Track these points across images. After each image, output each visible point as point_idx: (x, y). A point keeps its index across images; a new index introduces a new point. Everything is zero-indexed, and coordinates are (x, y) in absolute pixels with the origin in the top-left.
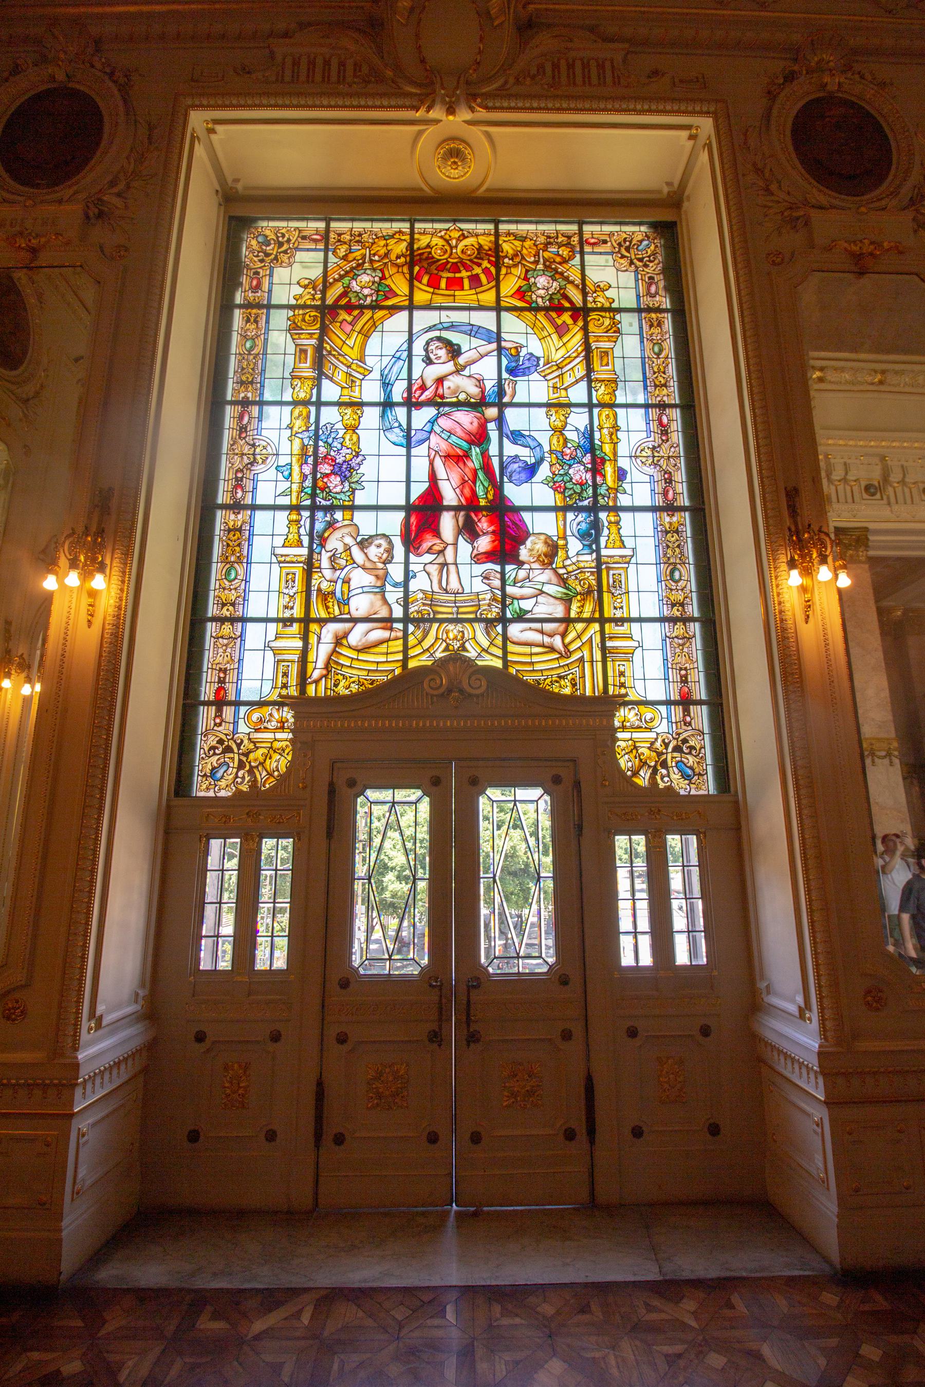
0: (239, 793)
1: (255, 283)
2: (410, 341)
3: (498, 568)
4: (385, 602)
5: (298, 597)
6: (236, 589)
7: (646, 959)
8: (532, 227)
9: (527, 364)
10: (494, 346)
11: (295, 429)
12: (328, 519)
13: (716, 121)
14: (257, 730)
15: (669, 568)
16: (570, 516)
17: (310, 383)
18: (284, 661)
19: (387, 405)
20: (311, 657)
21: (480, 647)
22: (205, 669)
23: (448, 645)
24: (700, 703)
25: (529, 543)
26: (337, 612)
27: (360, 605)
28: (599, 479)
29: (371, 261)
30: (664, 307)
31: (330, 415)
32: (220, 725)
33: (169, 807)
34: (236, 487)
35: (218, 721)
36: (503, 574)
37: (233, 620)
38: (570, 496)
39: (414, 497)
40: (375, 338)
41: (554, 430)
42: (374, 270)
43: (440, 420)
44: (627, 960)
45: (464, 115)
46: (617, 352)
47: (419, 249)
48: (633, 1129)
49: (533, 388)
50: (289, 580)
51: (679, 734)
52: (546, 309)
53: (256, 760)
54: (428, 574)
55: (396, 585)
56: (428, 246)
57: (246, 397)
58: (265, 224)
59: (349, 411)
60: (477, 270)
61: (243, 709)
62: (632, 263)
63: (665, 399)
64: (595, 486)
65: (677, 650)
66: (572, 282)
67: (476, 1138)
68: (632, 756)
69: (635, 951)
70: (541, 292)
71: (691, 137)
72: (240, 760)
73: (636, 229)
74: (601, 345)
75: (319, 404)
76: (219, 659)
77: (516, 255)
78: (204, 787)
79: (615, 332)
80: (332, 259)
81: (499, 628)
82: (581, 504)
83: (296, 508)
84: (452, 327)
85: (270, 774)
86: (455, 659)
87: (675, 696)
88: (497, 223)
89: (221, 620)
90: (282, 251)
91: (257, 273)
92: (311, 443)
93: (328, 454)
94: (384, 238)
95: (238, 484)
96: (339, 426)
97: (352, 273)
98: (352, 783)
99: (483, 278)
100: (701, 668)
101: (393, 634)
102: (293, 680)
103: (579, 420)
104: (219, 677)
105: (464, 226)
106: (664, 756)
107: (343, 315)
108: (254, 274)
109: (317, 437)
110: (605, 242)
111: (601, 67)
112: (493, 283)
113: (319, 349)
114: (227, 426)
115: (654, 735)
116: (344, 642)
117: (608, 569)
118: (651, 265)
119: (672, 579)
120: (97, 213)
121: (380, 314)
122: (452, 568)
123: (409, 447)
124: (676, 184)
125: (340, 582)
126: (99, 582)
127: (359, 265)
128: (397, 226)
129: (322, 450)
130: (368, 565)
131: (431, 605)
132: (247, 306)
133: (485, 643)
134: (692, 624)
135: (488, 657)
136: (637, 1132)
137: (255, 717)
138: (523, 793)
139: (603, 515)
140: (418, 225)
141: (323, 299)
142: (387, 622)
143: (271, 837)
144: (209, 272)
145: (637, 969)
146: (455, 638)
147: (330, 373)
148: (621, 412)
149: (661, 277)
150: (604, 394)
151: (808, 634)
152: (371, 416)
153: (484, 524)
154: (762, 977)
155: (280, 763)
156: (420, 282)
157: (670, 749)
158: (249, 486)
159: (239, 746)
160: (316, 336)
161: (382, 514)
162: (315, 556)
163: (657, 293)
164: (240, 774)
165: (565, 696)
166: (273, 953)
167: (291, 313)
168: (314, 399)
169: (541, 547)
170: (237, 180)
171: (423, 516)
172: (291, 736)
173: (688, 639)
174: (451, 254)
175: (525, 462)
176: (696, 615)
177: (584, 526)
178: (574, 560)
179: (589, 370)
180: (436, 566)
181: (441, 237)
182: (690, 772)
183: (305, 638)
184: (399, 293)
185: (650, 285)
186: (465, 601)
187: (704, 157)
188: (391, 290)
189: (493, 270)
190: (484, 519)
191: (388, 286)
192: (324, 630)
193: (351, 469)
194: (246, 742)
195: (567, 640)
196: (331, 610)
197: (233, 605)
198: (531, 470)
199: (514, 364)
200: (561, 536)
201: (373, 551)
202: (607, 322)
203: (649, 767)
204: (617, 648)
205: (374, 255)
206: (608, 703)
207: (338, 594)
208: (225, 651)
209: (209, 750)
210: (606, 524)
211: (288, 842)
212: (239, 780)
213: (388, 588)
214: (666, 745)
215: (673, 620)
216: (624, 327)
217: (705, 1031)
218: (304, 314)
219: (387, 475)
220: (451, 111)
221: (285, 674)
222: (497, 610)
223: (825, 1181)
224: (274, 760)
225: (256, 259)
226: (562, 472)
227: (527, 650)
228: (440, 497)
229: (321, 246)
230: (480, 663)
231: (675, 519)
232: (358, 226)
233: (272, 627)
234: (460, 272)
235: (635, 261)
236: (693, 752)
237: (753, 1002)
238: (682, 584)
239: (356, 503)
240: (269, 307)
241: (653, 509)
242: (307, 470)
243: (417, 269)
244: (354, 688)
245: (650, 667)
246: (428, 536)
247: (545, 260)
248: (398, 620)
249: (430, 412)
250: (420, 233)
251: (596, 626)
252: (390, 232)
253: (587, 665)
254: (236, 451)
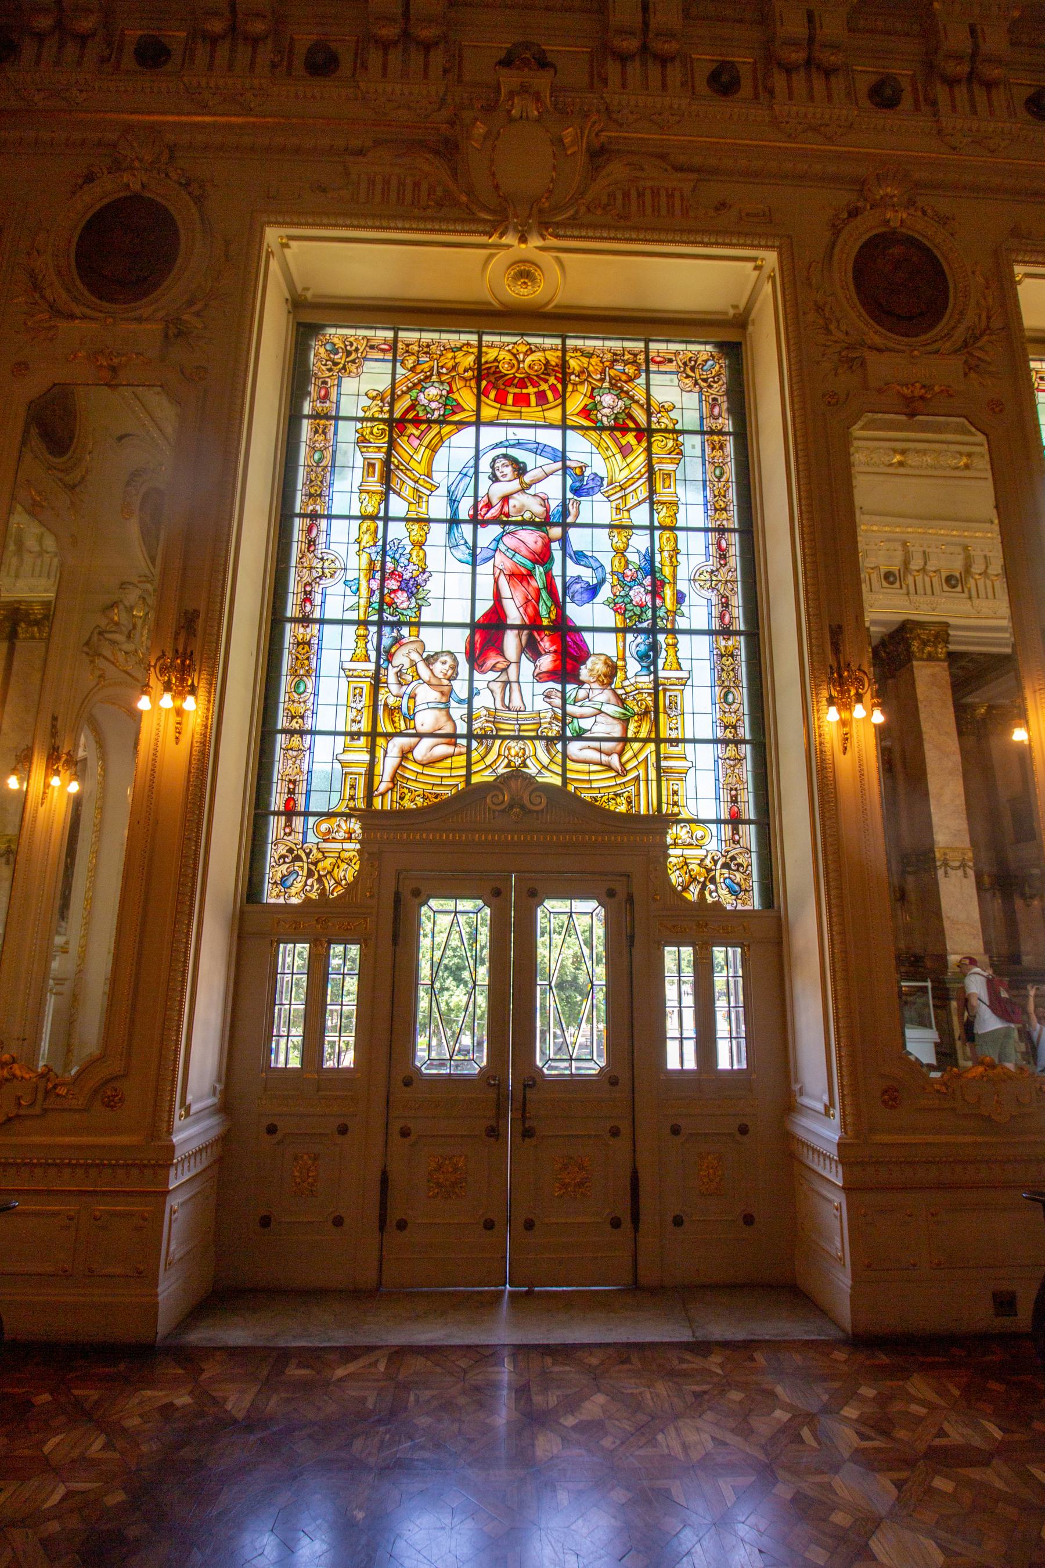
0: (308, 900)
1: (323, 393)
2: (477, 458)
3: (559, 687)
4: (450, 718)
5: (365, 711)
6: (305, 702)
7: (691, 1064)
8: (598, 343)
9: (591, 484)
10: (559, 465)
11: (363, 544)
12: (395, 634)
13: (780, 255)
14: (325, 841)
15: (725, 689)
16: (630, 637)
17: (378, 497)
18: (351, 773)
19: (454, 522)
20: (378, 770)
21: (541, 766)
22: (275, 780)
23: (510, 761)
24: (749, 822)
25: (589, 663)
26: (403, 727)
27: (426, 720)
28: (658, 601)
29: (439, 374)
30: (727, 430)
31: (397, 531)
32: (290, 834)
33: (242, 912)
34: (305, 600)
35: (288, 830)
36: (563, 692)
37: (302, 733)
38: (630, 618)
39: (479, 615)
40: (442, 452)
41: (617, 551)
42: (442, 383)
43: (504, 539)
44: (673, 1063)
45: (535, 242)
46: (679, 475)
47: (486, 363)
48: (675, 1217)
49: (596, 509)
50: (357, 694)
51: (728, 852)
52: (611, 429)
53: (324, 869)
54: (492, 692)
55: (460, 702)
56: (496, 360)
57: (314, 510)
58: (332, 331)
59: (416, 527)
60: (544, 387)
61: (312, 820)
62: (696, 383)
63: (725, 523)
64: (655, 609)
65: (729, 771)
66: (637, 402)
67: (529, 1225)
68: (682, 872)
69: (680, 1055)
70: (607, 411)
71: (756, 268)
72: (309, 869)
73: (701, 347)
74: (664, 466)
75: (387, 519)
76: (289, 771)
77: (583, 372)
78: (275, 894)
79: (678, 454)
80: (400, 370)
81: (559, 746)
82: (640, 626)
83: (365, 623)
84: (518, 445)
85: (338, 883)
86: (517, 775)
87: (725, 815)
88: (564, 338)
89: (291, 732)
90: (350, 360)
91: (326, 383)
92: (379, 558)
93: (395, 570)
94: (452, 350)
95: (307, 598)
96: (406, 541)
97: (420, 385)
98: (416, 893)
99: (550, 395)
100: (751, 789)
101: (457, 750)
102: (360, 793)
103: (640, 542)
104: (289, 788)
105: (531, 340)
106: (713, 873)
107: (411, 429)
108: (323, 383)
109: (384, 553)
110: (670, 361)
111: (671, 196)
112: (559, 401)
113: (387, 463)
114: (295, 539)
115: (702, 853)
116: (410, 756)
117: (665, 690)
118: (715, 385)
119: (726, 701)
120: (176, 332)
121: (447, 429)
122: (515, 686)
123: (474, 565)
124: (742, 308)
125: (406, 697)
126: (190, 704)
127: (427, 377)
128: (465, 338)
129: (390, 566)
130: (434, 681)
131: (493, 722)
132: (316, 416)
133: (546, 761)
134: (743, 746)
135: (548, 774)
136: (678, 1221)
137: (324, 827)
138: (579, 905)
139: (661, 638)
140: (485, 338)
141: (391, 412)
142: (452, 738)
143: (338, 942)
144: (279, 385)
145: (682, 1071)
146: (517, 755)
147: (397, 488)
148: (681, 535)
149: (725, 398)
150: (665, 517)
151: (844, 764)
152: (438, 531)
153: (546, 644)
154: (797, 1081)
155: (348, 873)
156: (487, 397)
157: (718, 866)
158: (317, 599)
159: (308, 855)
160: (384, 450)
161: (446, 630)
162: (382, 671)
163: (720, 415)
164: (309, 882)
165: (620, 813)
166: (342, 1052)
167: (359, 425)
168: (382, 514)
169: (601, 668)
170: (307, 289)
171: (487, 633)
172: (358, 846)
173: (739, 760)
174: (519, 368)
175: (587, 582)
176: (748, 737)
177: (642, 648)
178: (633, 681)
179: (652, 491)
180: (500, 684)
181: (509, 351)
182: (737, 888)
183: (372, 752)
184: (467, 408)
185: (713, 407)
186: (526, 719)
187: (768, 288)
188: (459, 404)
189: (559, 387)
190: (546, 639)
191: (456, 400)
192: (390, 744)
193: (417, 585)
194: (315, 851)
195: (624, 759)
196: (397, 725)
197: (302, 717)
198: (593, 591)
199: (578, 484)
200: (621, 656)
201: (438, 668)
202: (671, 443)
203: (699, 882)
204: (671, 768)
205: (442, 367)
206: (661, 821)
207: (404, 710)
208: (294, 763)
209: (280, 858)
210: (664, 646)
211: (354, 950)
212: (308, 888)
213: (453, 704)
214: (716, 862)
215: (726, 742)
216: (687, 450)
217: (743, 1130)
218: (372, 427)
219: (453, 590)
220: (523, 239)
221: (353, 787)
222: (557, 728)
223: (842, 1259)
224: (341, 869)
225: (324, 368)
226: (623, 593)
227: (585, 767)
228: (504, 616)
229: (389, 356)
230: (540, 780)
231: (730, 643)
232: (427, 336)
233: (340, 739)
234: (527, 387)
235: (700, 381)
236: (741, 869)
237: (788, 1104)
238: (735, 707)
239: (422, 620)
240: (337, 418)
241: (709, 632)
242: (375, 585)
243: (484, 383)
244: (419, 801)
245: (702, 786)
246: (492, 654)
247: (611, 378)
248: (462, 736)
249: (496, 530)
250: (488, 346)
251: (652, 746)
252: (458, 345)
253: (642, 784)
254: (305, 565)
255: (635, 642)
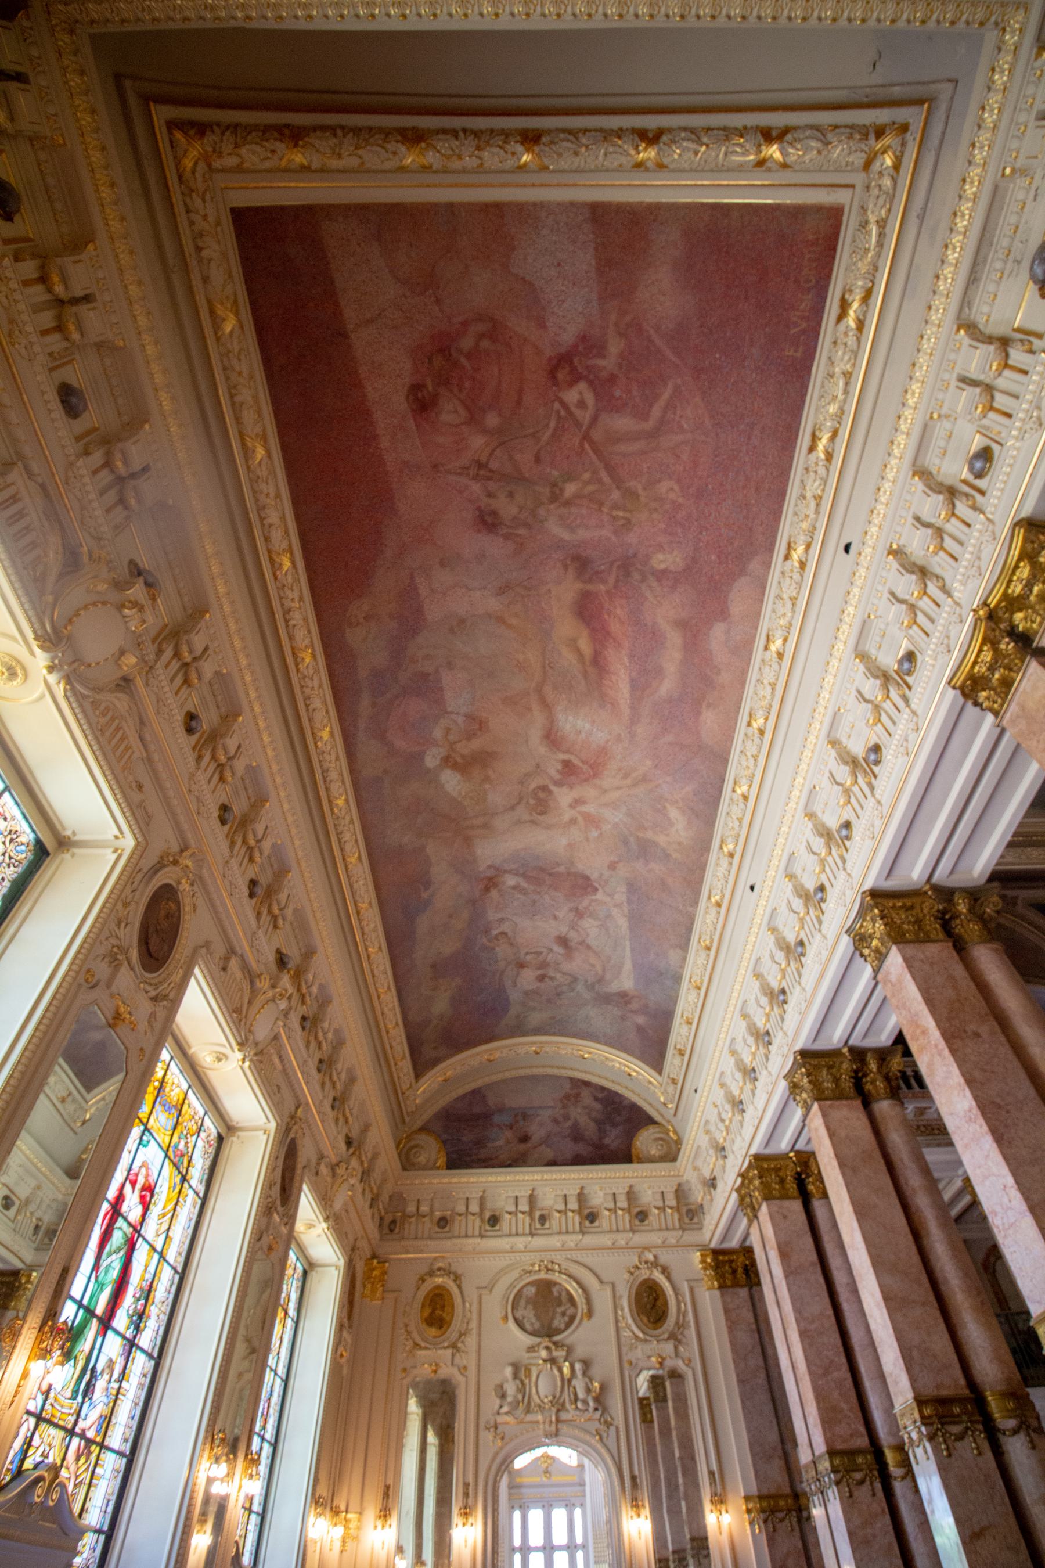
71: (116, 837)
124: (76, 838)
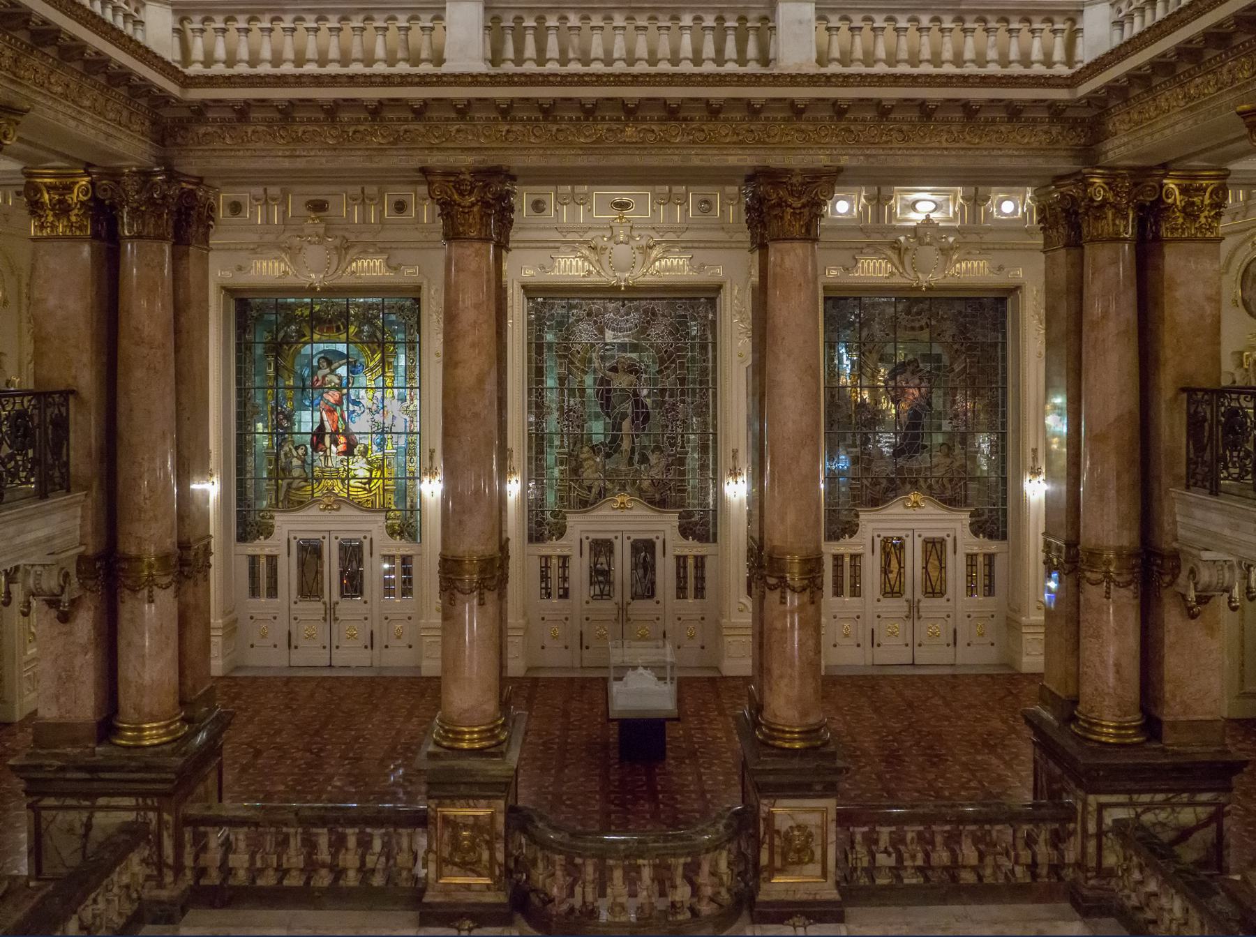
142: (306, 480)
201: (301, 451)
255: (377, 438)
